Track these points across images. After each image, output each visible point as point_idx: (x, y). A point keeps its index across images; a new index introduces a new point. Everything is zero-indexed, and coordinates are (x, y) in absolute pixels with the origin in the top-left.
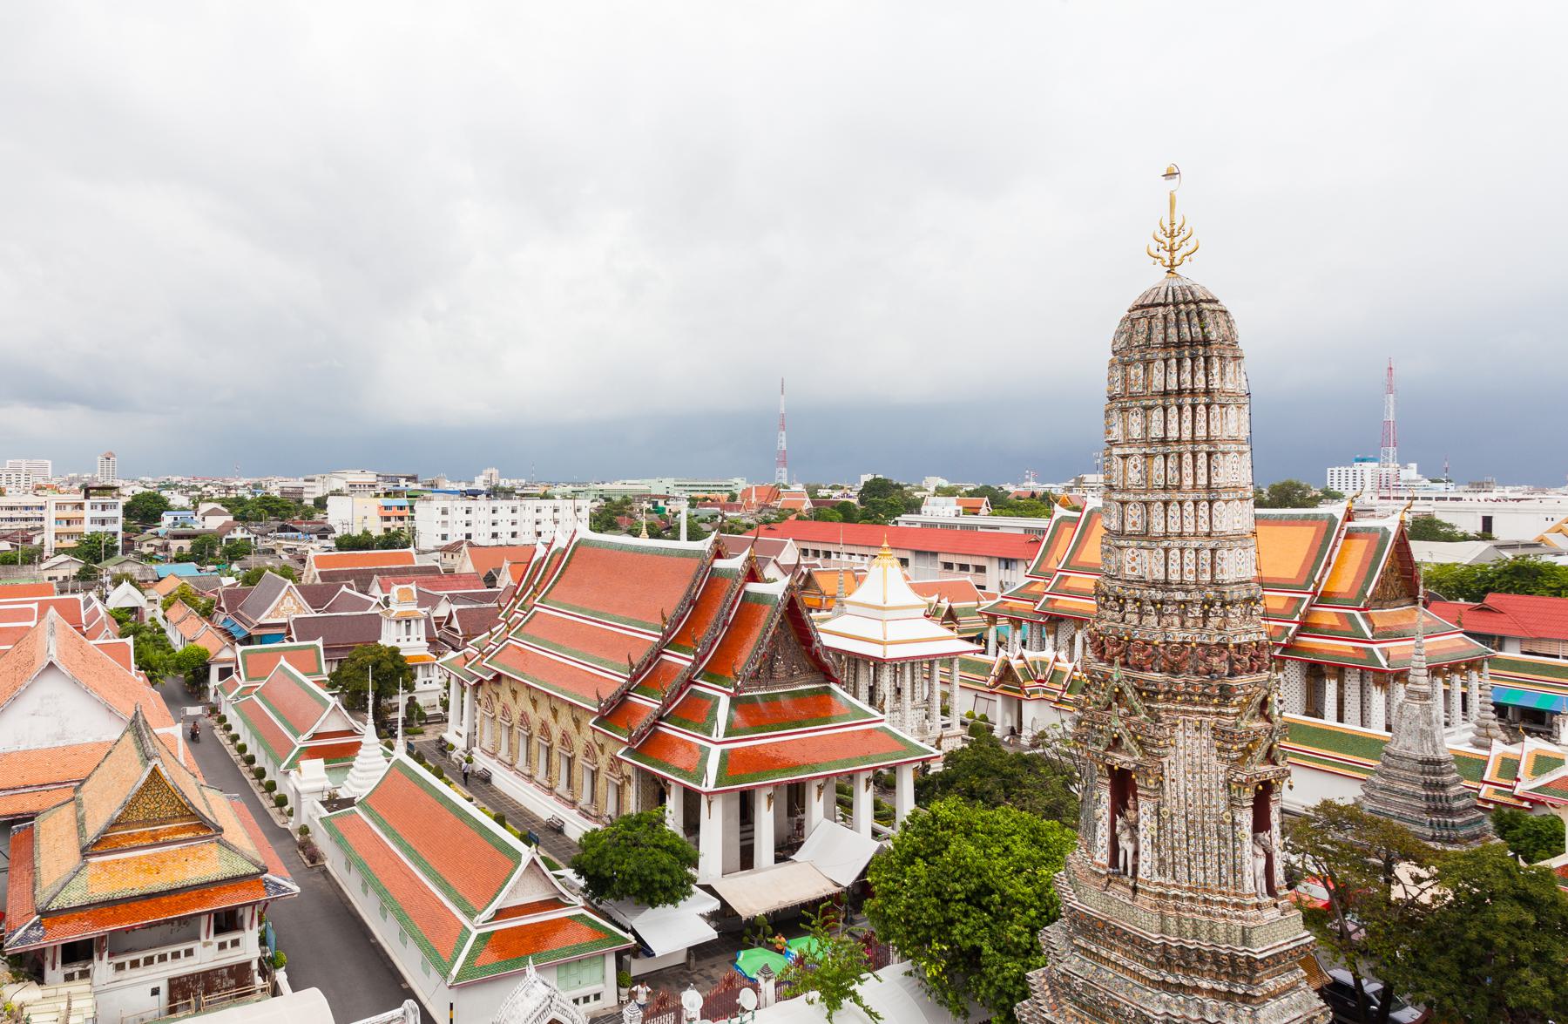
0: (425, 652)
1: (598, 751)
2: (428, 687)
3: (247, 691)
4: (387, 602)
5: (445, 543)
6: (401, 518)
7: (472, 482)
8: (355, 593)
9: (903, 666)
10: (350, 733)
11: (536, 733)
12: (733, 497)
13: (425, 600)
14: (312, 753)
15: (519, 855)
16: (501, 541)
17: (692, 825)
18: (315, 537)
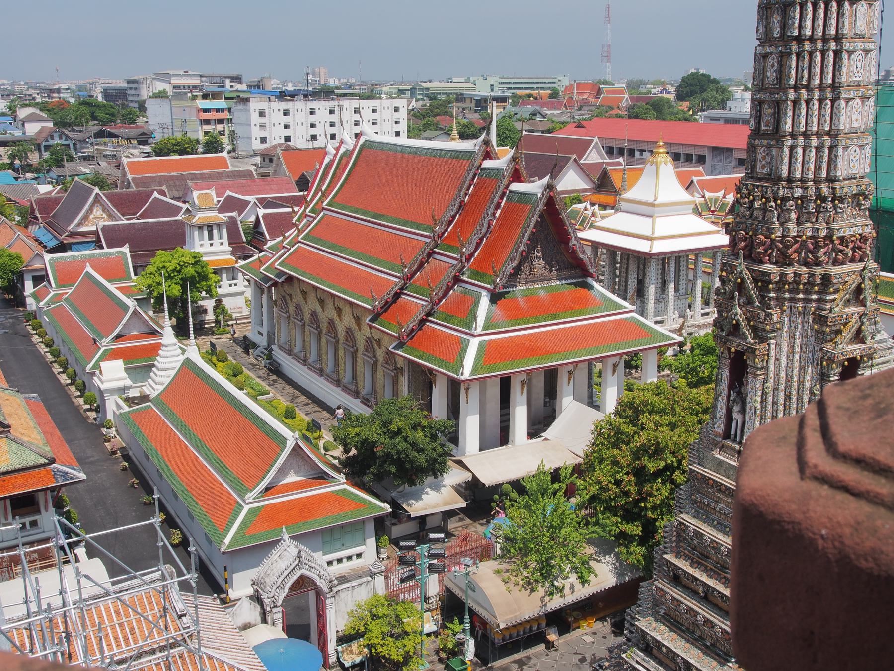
0: (229, 257)
1: (376, 346)
3: (57, 298)
9: (669, 259)
12: (554, 95)
17: (454, 411)
18: (135, 142)
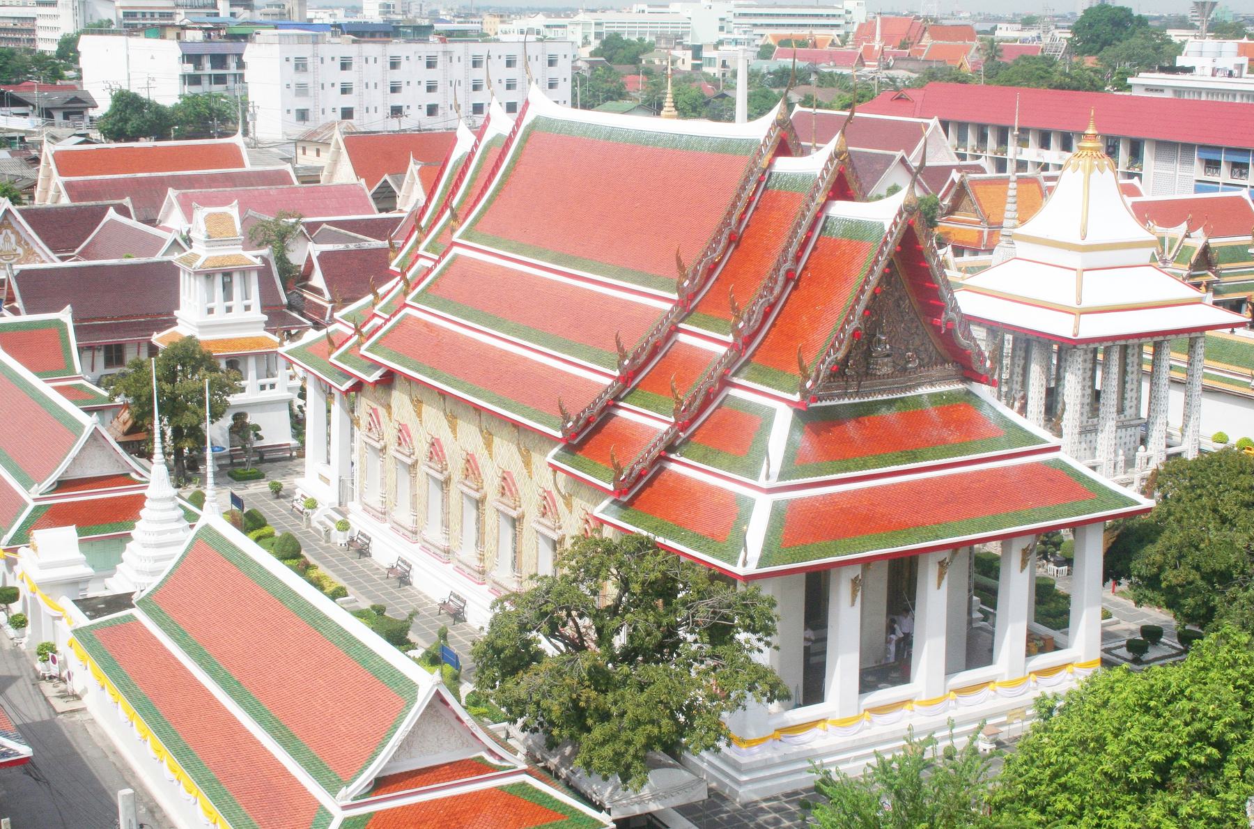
2: (268, 395)
8: (132, 223)
10: (123, 479)
11: (457, 476)
14: (55, 516)
15: (412, 687)
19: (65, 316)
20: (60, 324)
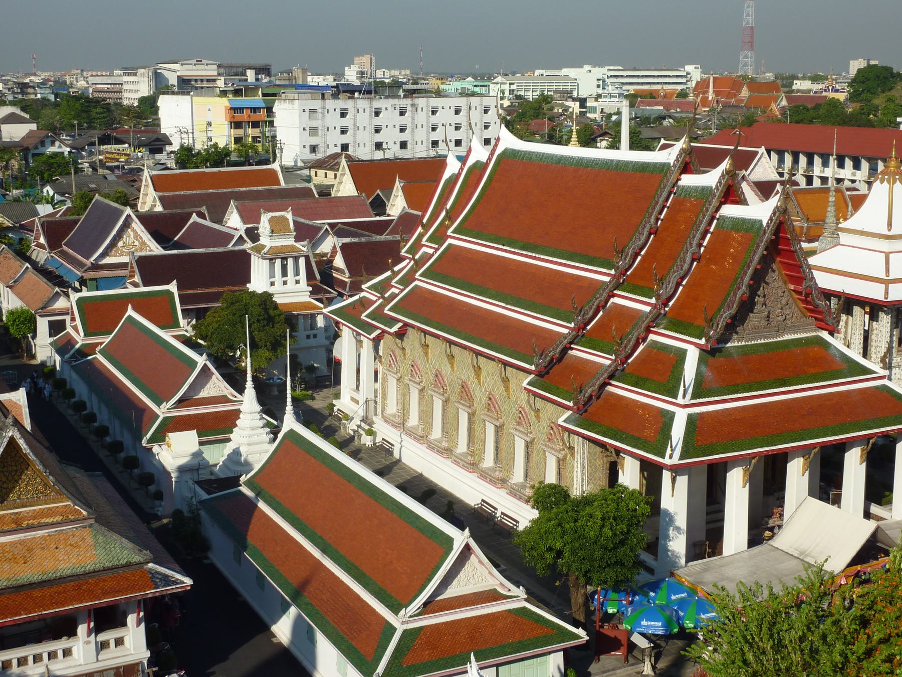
4: (253, 235)
5: (313, 157)
6: (255, 125)
7: (339, 75)
10: (224, 399)
13: (304, 232)
16: (389, 155)
19: (173, 287)
20: (169, 293)
